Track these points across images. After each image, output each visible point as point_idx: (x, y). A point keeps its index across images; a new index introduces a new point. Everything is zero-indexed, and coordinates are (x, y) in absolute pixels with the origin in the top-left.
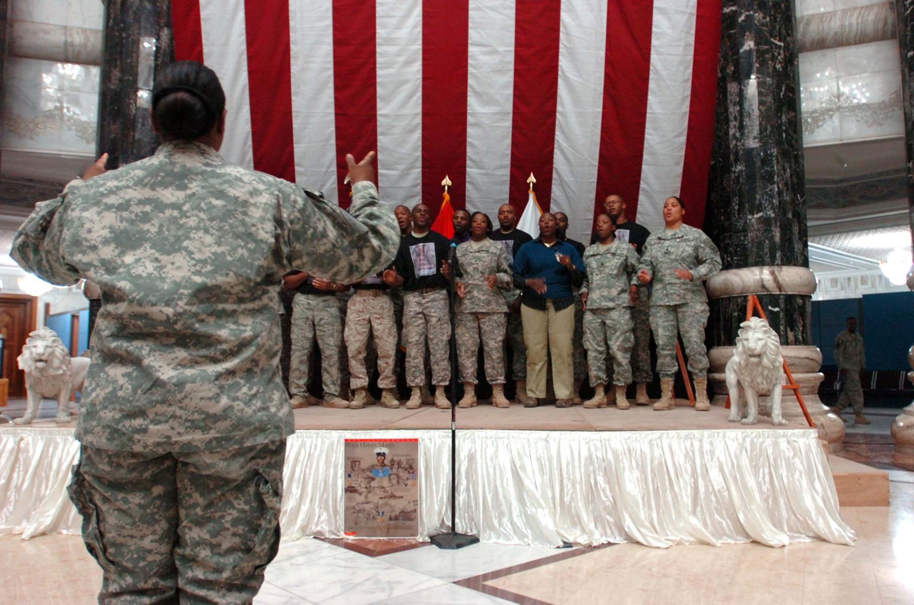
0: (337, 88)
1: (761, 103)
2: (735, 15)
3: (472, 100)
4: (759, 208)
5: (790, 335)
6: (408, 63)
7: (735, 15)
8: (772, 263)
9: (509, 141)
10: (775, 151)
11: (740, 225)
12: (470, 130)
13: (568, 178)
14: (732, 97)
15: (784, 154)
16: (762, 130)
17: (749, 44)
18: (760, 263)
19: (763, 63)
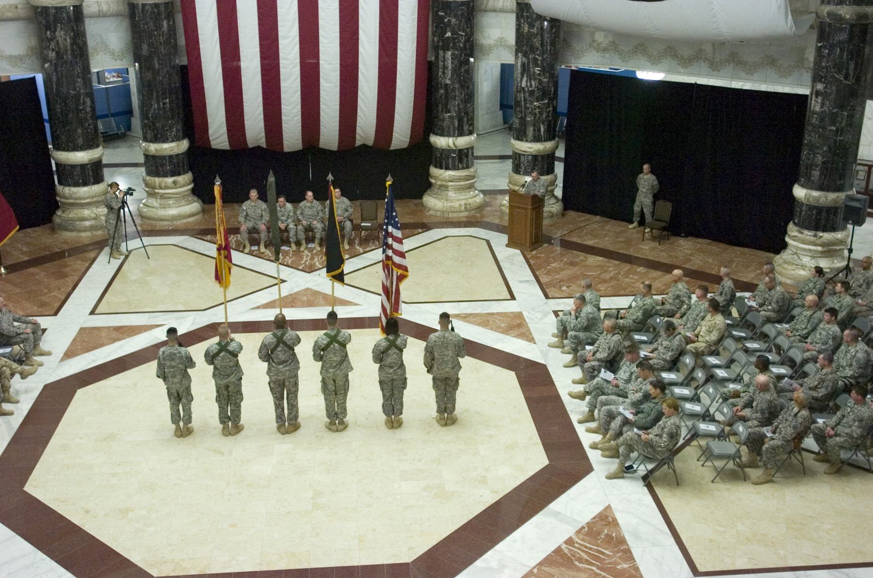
0: (263, 75)
1: (452, 63)
2: (442, 18)
3: (321, 81)
4: (449, 111)
5: (460, 166)
6: (294, 67)
7: (442, 18)
8: (454, 136)
9: (338, 96)
10: (457, 86)
11: (441, 117)
12: (321, 92)
13: (364, 109)
14: (441, 58)
15: (462, 86)
16: (452, 75)
17: (449, 34)
18: (449, 136)
19: (454, 44)
